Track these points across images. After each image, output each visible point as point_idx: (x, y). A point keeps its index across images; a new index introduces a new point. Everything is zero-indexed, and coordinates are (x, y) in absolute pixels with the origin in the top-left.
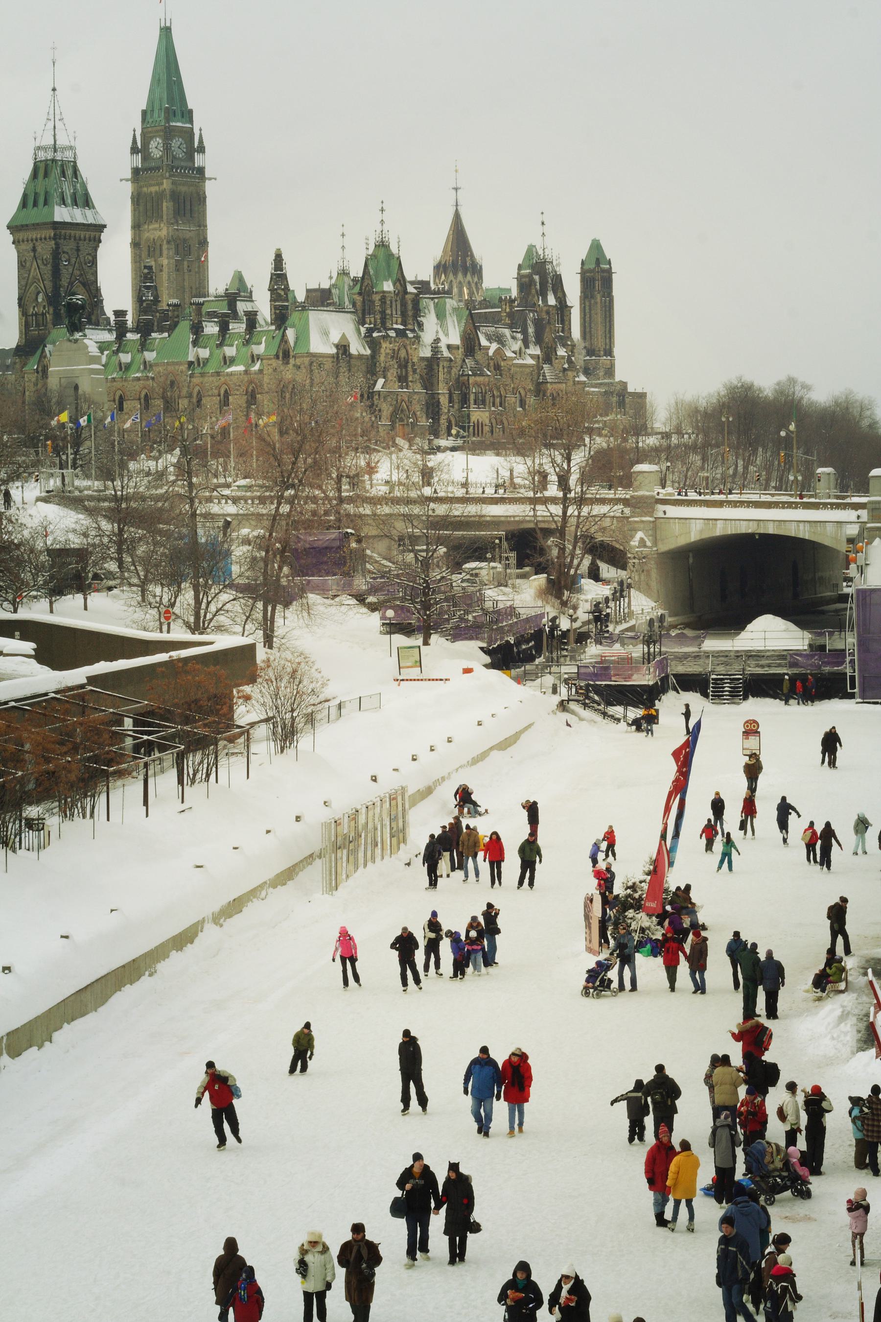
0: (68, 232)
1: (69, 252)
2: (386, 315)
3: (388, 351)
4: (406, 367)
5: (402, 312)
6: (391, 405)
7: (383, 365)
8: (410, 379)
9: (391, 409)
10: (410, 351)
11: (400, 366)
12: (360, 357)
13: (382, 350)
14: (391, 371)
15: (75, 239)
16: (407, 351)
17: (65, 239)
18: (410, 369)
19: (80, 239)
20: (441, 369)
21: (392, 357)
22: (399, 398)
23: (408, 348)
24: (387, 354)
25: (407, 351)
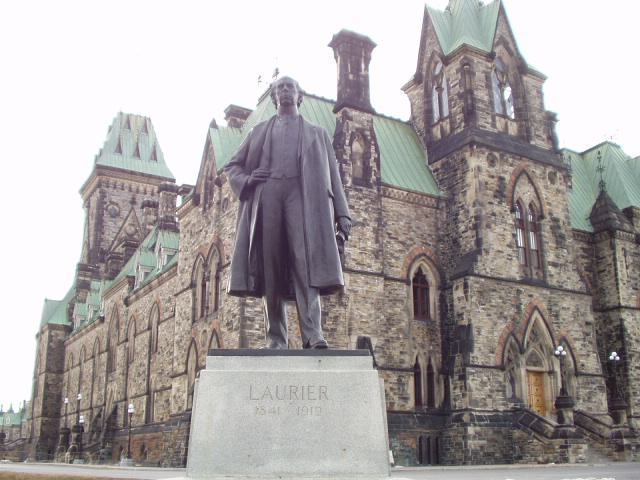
0: (119, 182)
1: (121, 204)
2: (474, 99)
3: (484, 177)
4: (537, 229)
5: (517, 110)
6: (501, 316)
7: (472, 213)
8: (550, 257)
9: (502, 326)
10: (544, 193)
11: (521, 224)
12: (414, 199)
13: (470, 177)
14: (498, 229)
15: (130, 190)
16: (536, 190)
17: (115, 187)
18: (547, 233)
19: (138, 191)
20: (619, 254)
21: (500, 194)
22: (525, 300)
23: (540, 184)
24: (483, 186)
25: (536, 190)
